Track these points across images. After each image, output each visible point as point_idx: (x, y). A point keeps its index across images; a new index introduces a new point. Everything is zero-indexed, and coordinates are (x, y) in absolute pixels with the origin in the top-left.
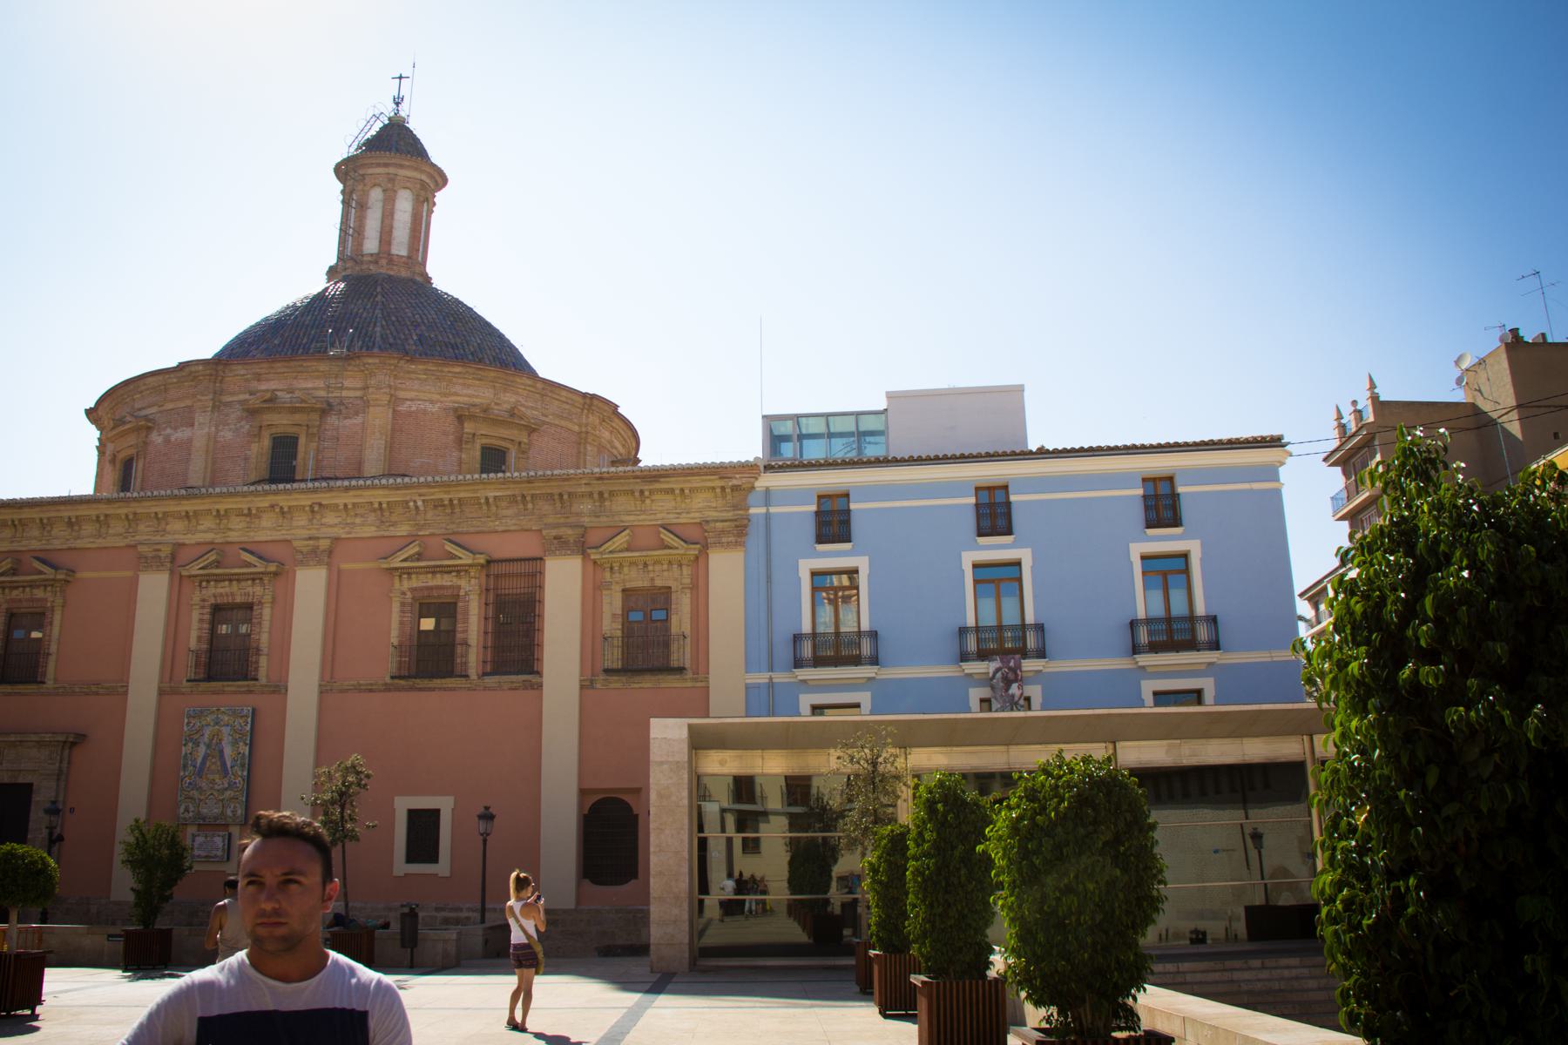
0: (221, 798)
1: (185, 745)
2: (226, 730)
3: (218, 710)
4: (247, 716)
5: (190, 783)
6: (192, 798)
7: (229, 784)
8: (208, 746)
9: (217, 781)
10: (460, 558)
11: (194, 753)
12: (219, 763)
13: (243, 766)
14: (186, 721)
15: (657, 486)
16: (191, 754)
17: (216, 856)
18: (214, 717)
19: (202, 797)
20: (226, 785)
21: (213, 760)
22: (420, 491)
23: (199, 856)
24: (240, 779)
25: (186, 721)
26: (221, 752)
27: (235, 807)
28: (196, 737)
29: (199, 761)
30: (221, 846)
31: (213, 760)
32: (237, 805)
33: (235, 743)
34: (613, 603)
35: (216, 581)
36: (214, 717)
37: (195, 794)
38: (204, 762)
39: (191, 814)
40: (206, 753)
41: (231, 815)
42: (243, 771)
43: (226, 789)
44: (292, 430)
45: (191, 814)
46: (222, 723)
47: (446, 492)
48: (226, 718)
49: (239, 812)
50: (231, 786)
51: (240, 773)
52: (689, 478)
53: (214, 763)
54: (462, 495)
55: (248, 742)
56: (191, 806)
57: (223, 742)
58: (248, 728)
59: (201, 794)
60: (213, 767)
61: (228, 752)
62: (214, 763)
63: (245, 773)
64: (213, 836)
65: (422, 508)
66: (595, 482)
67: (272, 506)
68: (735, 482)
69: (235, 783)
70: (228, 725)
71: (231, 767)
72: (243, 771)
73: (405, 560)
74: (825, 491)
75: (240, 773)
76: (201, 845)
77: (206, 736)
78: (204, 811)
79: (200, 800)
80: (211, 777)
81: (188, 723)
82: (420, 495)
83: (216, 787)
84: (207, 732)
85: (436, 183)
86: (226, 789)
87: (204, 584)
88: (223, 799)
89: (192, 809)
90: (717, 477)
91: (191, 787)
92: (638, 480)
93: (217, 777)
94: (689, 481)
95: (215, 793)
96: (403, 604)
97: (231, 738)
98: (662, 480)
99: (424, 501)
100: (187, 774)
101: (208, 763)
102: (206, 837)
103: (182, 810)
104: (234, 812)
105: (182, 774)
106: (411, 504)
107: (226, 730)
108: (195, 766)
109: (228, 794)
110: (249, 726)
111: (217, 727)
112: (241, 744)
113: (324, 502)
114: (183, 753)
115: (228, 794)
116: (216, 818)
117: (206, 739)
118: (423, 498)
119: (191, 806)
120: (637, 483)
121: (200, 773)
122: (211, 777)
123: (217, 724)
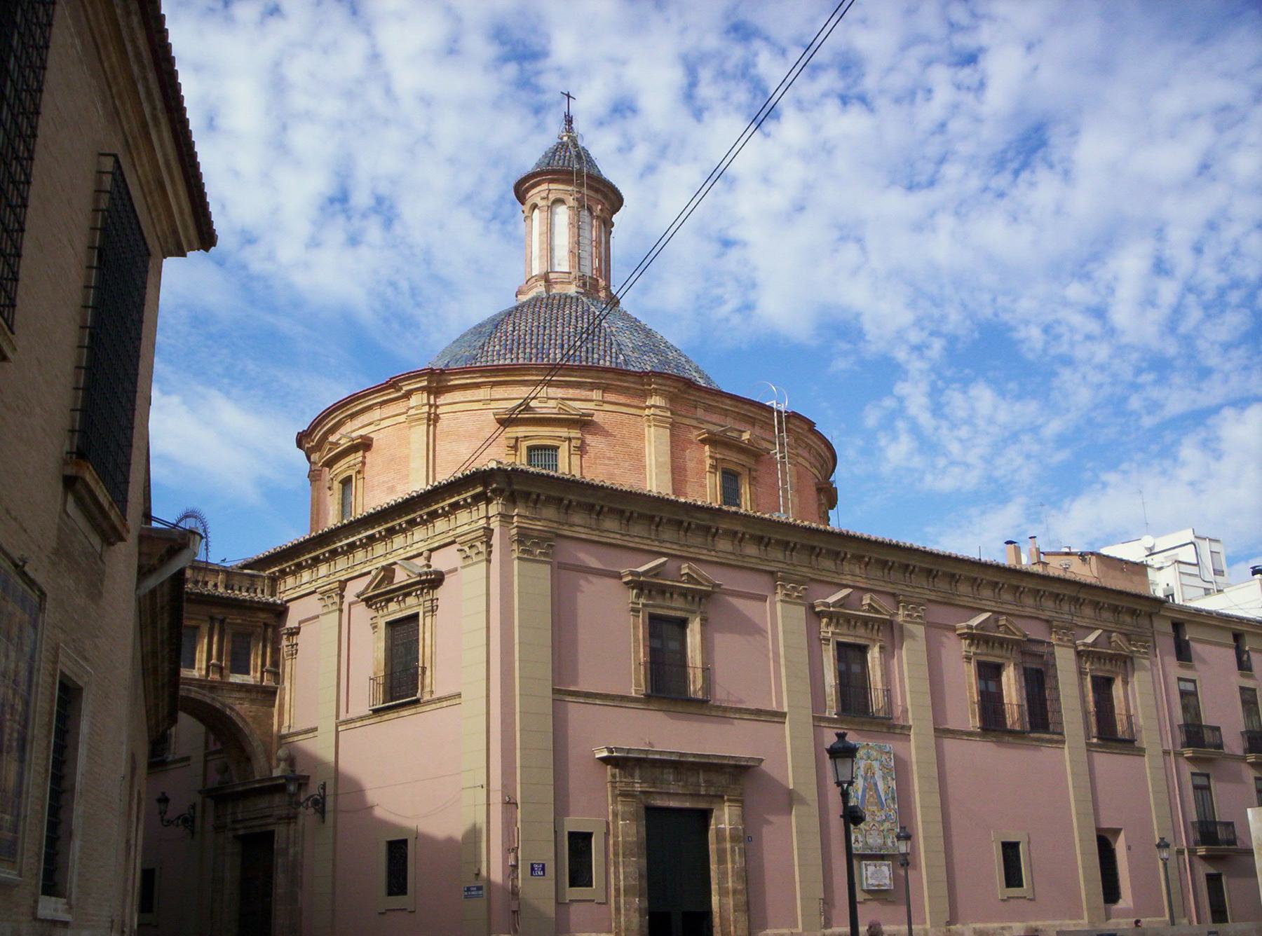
0: (882, 828)
2: (876, 765)
8: (865, 779)
13: (893, 799)
17: (885, 885)
18: (865, 751)
19: (868, 828)
20: (884, 818)
23: (872, 885)
26: (876, 784)
29: (860, 793)
30: (888, 875)
33: (884, 778)
36: (865, 751)
38: (864, 796)
42: (894, 804)
43: (884, 821)
44: (739, 469)
45: (861, 845)
48: (875, 754)
50: (887, 818)
53: (872, 796)
56: (859, 836)
58: (893, 764)
60: (871, 800)
63: (896, 807)
64: (880, 866)
70: (877, 760)
75: (892, 806)
76: (873, 874)
77: (862, 769)
78: (870, 841)
79: (866, 831)
83: (877, 819)
86: (884, 821)
88: (883, 831)
89: (860, 839)
93: (874, 808)
101: (867, 796)
102: (875, 866)
107: (874, 763)
108: (857, 798)
109: (886, 825)
111: (869, 761)
115: (886, 825)
119: (859, 836)
123: (869, 758)
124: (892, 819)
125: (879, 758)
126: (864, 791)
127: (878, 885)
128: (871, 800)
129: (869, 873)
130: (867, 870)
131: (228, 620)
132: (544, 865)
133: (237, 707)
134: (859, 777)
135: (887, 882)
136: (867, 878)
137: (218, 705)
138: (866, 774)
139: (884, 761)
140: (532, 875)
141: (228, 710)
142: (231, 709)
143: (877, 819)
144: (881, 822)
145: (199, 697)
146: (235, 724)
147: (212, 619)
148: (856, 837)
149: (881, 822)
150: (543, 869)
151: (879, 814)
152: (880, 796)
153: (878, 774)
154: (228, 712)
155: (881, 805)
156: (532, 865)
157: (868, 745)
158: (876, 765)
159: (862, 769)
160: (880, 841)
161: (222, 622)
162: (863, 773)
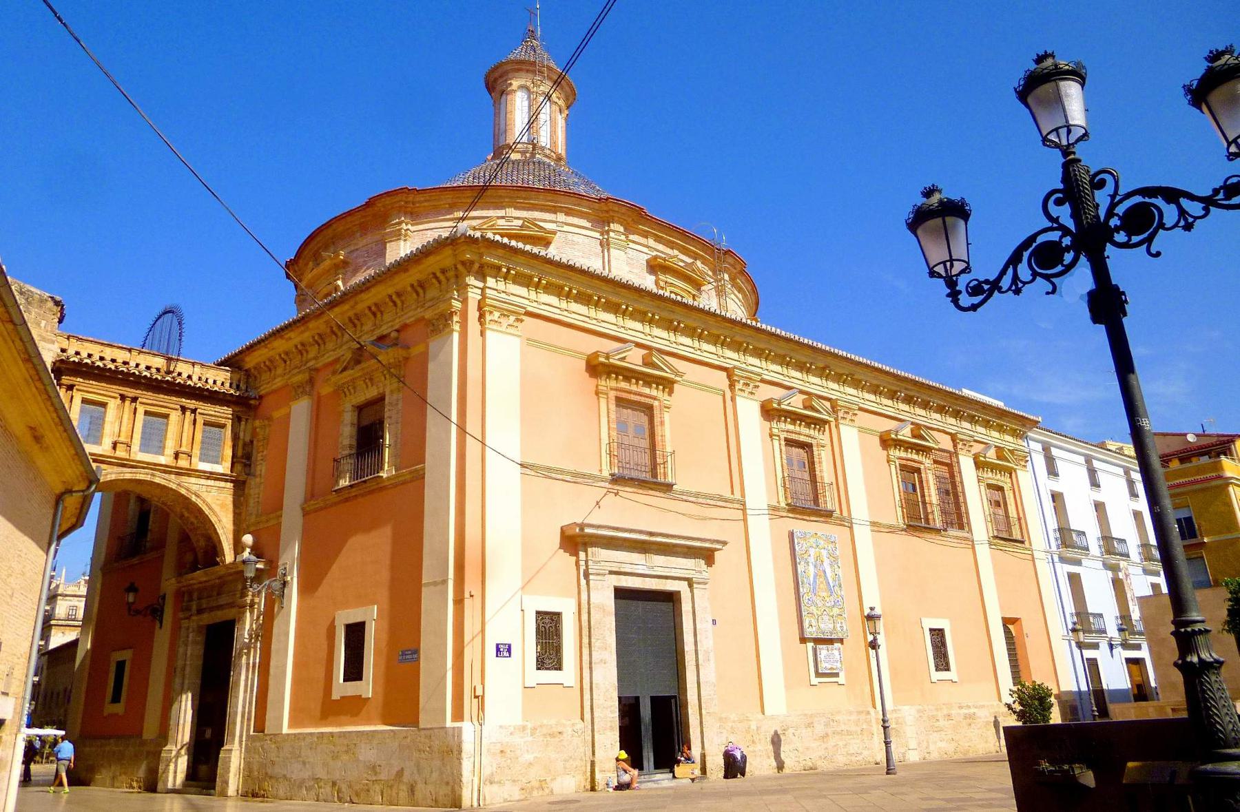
0: (831, 614)
2: (824, 553)
10: (929, 442)
14: (796, 541)
19: (819, 613)
20: (833, 603)
26: (825, 572)
32: (843, 621)
33: (831, 565)
37: (815, 612)
38: (815, 581)
39: (814, 628)
41: (839, 629)
53: (822, 583)
61: (828, 571)
62: (822, 583)
78: (822, 626)
81: (798, 543)
83: (828, 605)
84: (812, 552)
89: (814, 624)
91: (810, 602)
93: (825, 594)
105: (801, 590)
115: (836, 611)
117: (811, 560)
124: (840, 605)
125: (826, 547)
126: (816, 575)
127: (831, 669)
129: (822, 656)
131: (199, 410)
132: (510, 646)
133: (204, 495)
134: (810, 564)
137: (183, 491)
139: (831, 551)
140: (497, 656)
141: (193, 496)
142: (198, 496)
145: (163, 482)
146: (200, 511)
147: (184, 409)
148: (810, 621)
150: (509, 650)
154: (194, 498)
156: (497, 645)
158: (824, 553)
161: (194, 411)
162: (813, 560)
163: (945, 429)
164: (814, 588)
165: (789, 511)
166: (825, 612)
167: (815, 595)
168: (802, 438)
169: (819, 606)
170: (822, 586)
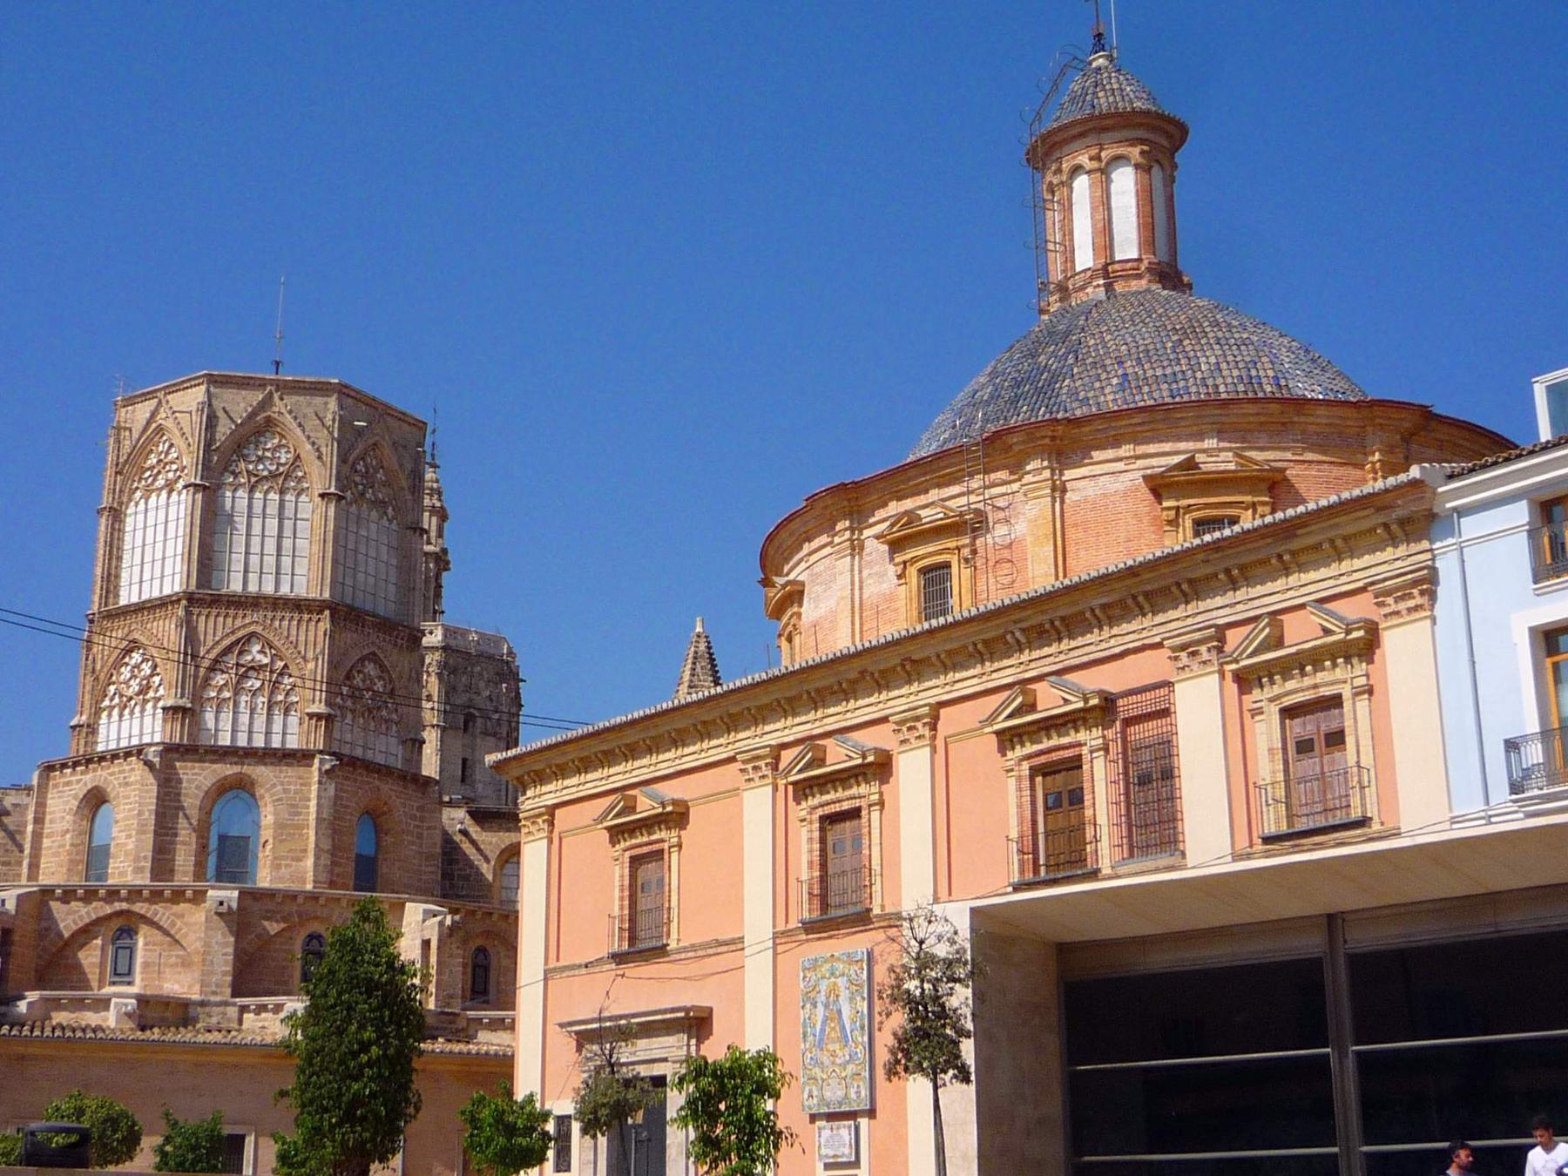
0: (843, 1075)
1: (803, 1007)
2: (842, 982)
3: (833, 956)
4: (862, 960)
5: (812, 1058)
6: (815, 1079)
7: (850, 1055)
8: (826, 1006)
9: (838, 1051)
11: (813, 1016)
12: (837, 1028)
15: (1295, 544)
16: (809, 1018)
18: (828, 966)
19: (825, 1077)
20: (848, 1057)
21: (832, 1025)
22: (1013, 618)
24: (860, 1047)
25: (802, 975)
26: (839, 1012)
27: (858, 1086)
28: (812, 995)
29: (818, 1027)
31: (832, 1025)
34: (1267, 732)
35: (819, 785)
36: (828, 966)
37: (817, 1071)
38: (823, 1030)
39: (815, 1100)
40: (825, 1016)
41: (853, 1096)
42: (862, 1037)
43: (848, 1062)
45: (815, 1100)
46: (838, 973)
47: (1042, 612)
49: (863, 1093)
51: (860, 1039)
52: (1337, 520)
53: (834, 1029)
54: (1063, 612)
55: (865, 995)
56: (814, 1088)
57: (840, 999)
58: (865, 976)
59: (823, 1072)
63: (866, 1038)
64: (838, 1128)
65: (1023, 640)
66: (1216, 556)
67: (863, 673)
68: (1400, 513)
69: (856, 1053)
70: (843, 975)
71: (852, 1031)
72: (862, 1036)
73: (1010, 716)
74: (1547, 495)
75: (860, 1039)
76: (828, 1141)
77: (823, 993)
78: (828, 1094)
79: (823, 1080)
80: (831, 1047)
81: (804, 977)
82: (1015, 622)
83: (838, 1061)
85: (1169, 136)
86: (848, 1062)
87: (807, 791)
88: (845, 1078)
89: (815, 1093)
90: (1372, 510)
92: (1269, 540)
93: (837, 1046)
94: (1337, 525)
95: (837, 1070)
96: (1019, 779)
97: (847, 992)
98: (1299, 532)
99: (1023, 630)
100: (807, 1046)
101: (827, 1030)
103: (806, 1096)
104: (858, 1093)
106: (1009, 637)
107: (842, 982)
108: (815, 1035)
109: (851, 1068)
110: (865, 972)
111: (833, 979)
112: (858, 998)
113: (915, 657)
114: (802, 1020)
115: (851, 1068)
116: (840, 1104)
117: (822, 998)
118: (1019, 626)
119: (814, 1088)
120: (1268, 544)
121: (820, 1045)
122: (831, 1047)
124: (859, 1059)
126: (824, 1022)
127: (835, 1156)
128: (833, 1035)
130: (820, 1136)
135: (847, 1151)
136: (820, 1146)
138: (828, 998)
139: (854, 976)
143: (838, 1061)
144: (844, 1066)
148: (810, 1091)
149: (844, 1066)
151: (841, 1054)
152: (844, 1027)
153: (844, 995)
155: (844, 1039)
157: (833, 956)
159: (823, 993)
160: (840, 1093)
162: (823, 999)
163: (1146, 641)
164: (821, 1040)
165: (807, 932)
166: (834, 1074)
167: (822, 1049)
168: (846, 806)
169: (826, 1064)
170: (833, 1035)
